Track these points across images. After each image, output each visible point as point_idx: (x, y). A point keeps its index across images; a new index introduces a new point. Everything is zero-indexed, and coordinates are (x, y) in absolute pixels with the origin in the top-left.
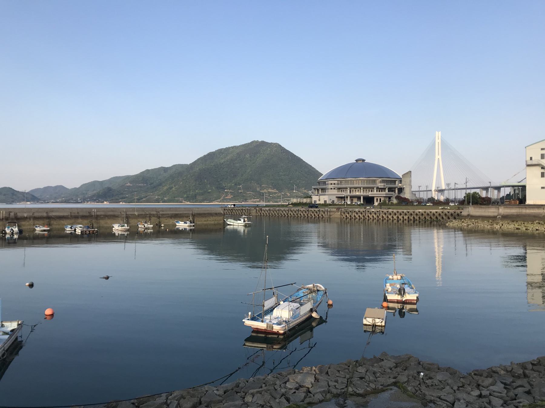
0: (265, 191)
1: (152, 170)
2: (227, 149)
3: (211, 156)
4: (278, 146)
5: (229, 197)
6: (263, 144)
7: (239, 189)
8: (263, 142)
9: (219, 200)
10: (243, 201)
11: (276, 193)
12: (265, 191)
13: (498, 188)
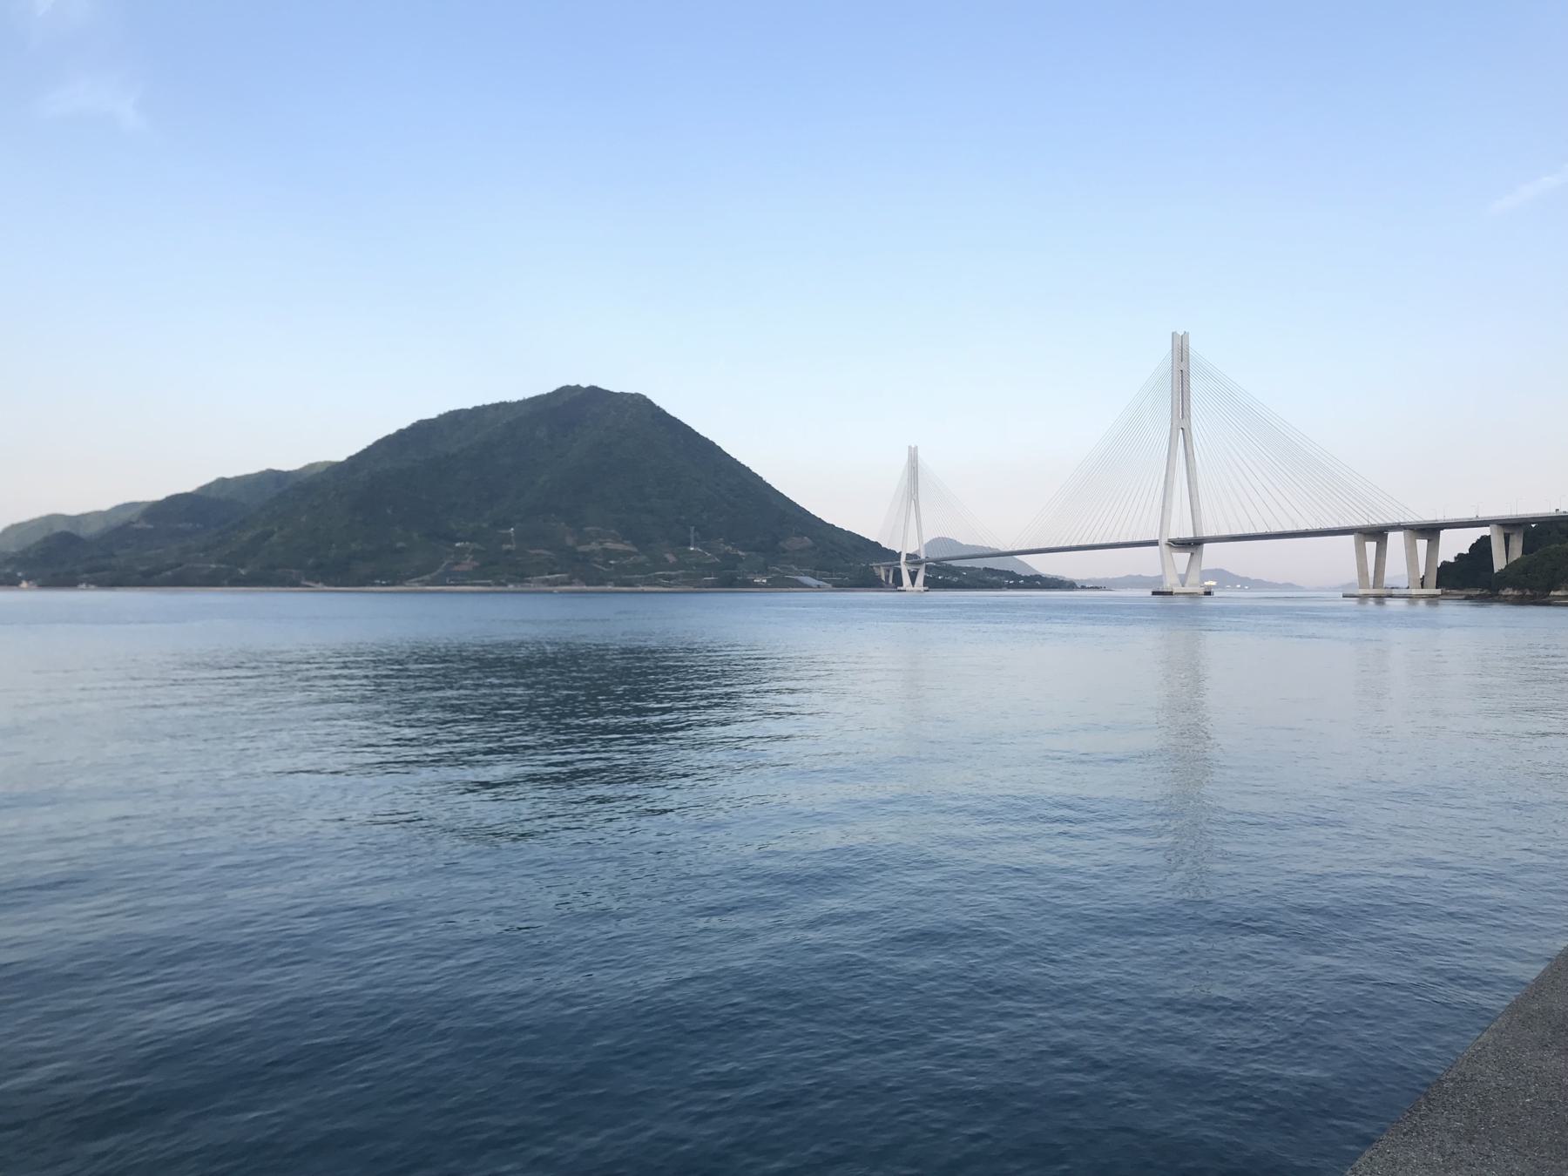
0: (594, 546)
1: (237, 479)
3: (422, 430)
5: (468, 564)
6: (595, 394)
7: (507, 539)
8: (594, 391)
9: (427, 577)
11: (628, 554)
12: (594, 546)
13: (1430, 532)
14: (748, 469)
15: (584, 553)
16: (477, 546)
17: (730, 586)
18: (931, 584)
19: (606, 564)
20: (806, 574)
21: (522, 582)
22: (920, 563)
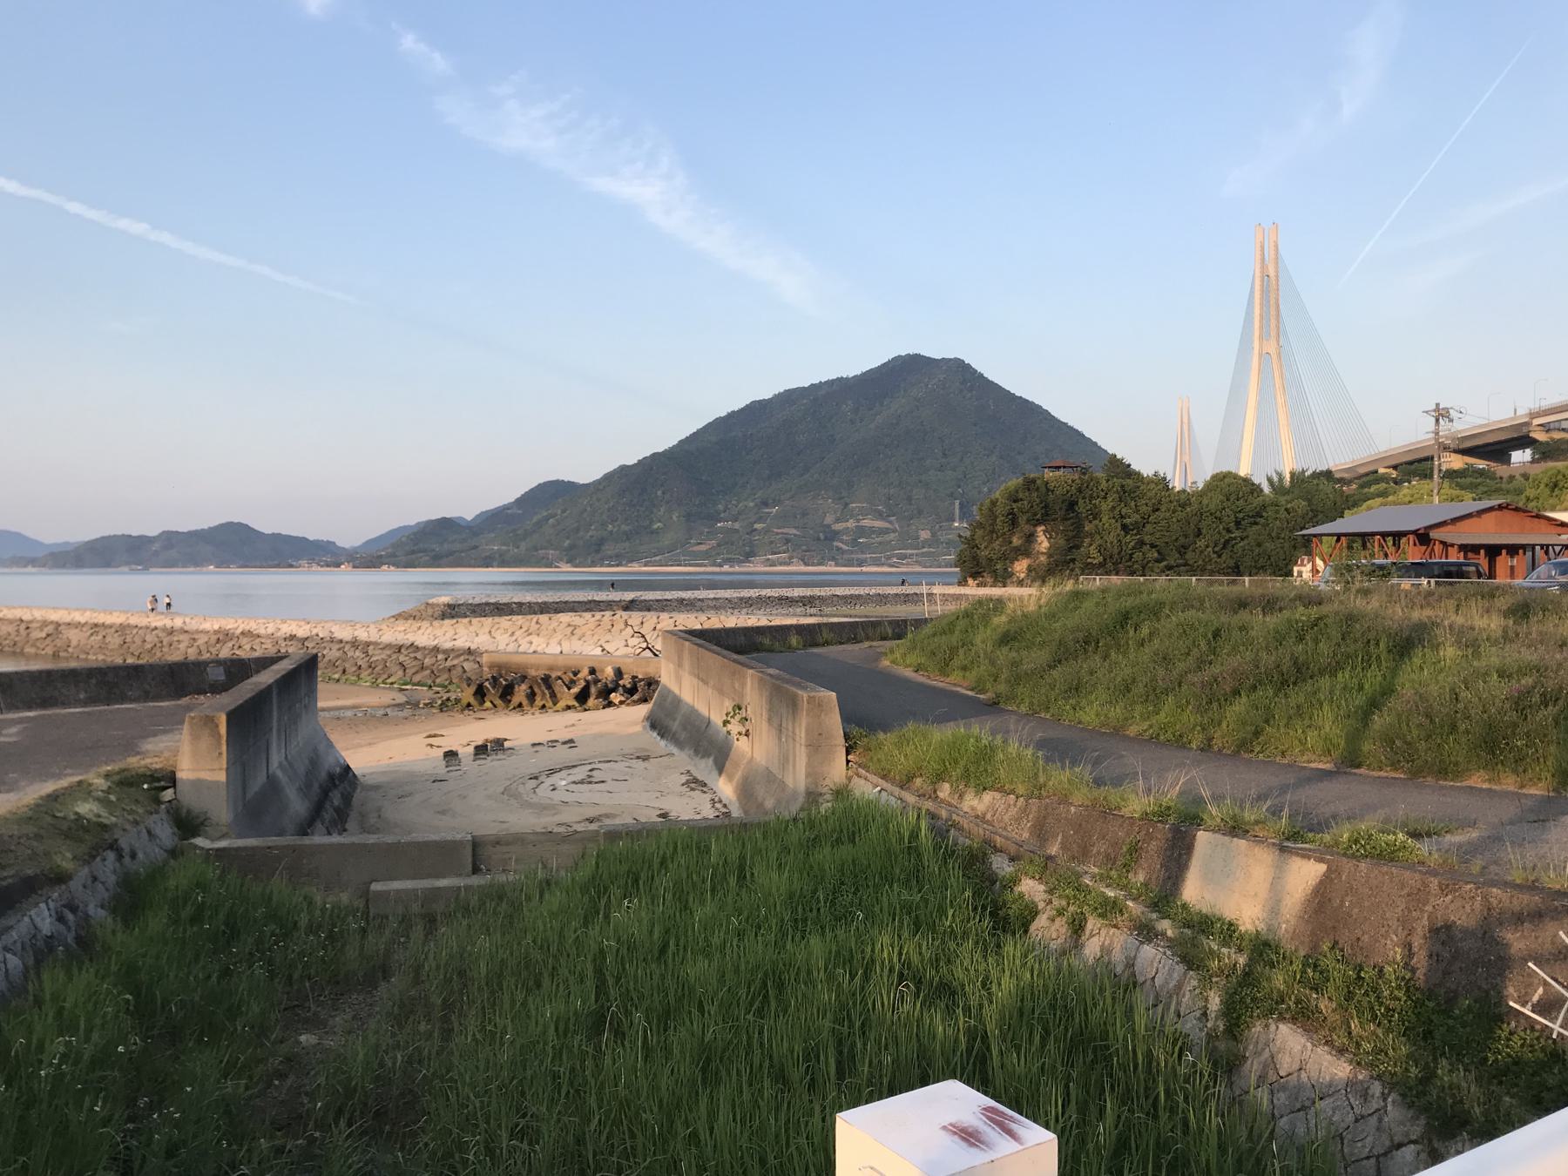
3: (755, 411)
4: (959, 370)
5: (703, 548)
10: (728, 561)
12: (851, 524)
15: (837, 533)
19: (854, 542)
21: (740, 562)
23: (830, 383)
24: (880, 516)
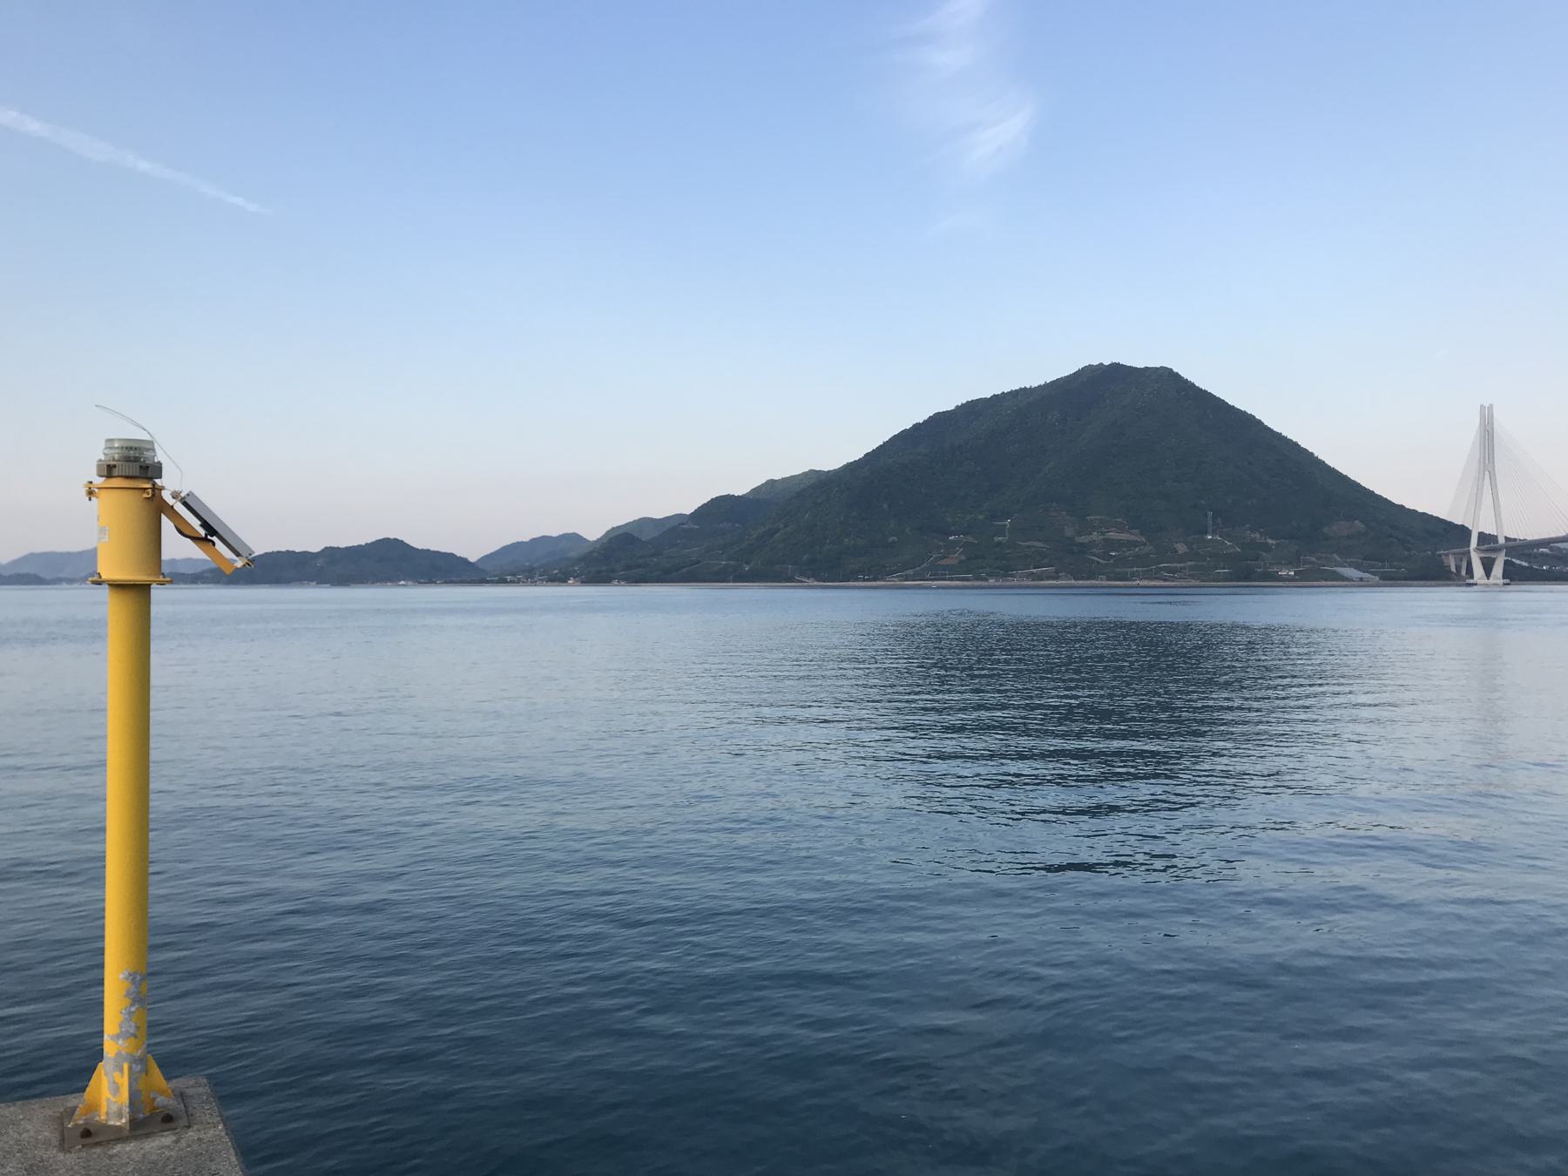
1: (784, 480)
2: (997, 400)
3: (939, 422)
4: (1166, 378)
5: (952, 560)
6: (1115, 374)
8: (1116, 367)
9: (910, 572)
10: (991, 575)
11: (1135, 544)
12: (1095, 536)
14: (1296, 444)
16: (970, 539)
17: (1247, 579)
18: (1514, 575)
20: (1350, 565)
22: (1497, 550)
23: (1014, 394)
24: (1122, 531)
